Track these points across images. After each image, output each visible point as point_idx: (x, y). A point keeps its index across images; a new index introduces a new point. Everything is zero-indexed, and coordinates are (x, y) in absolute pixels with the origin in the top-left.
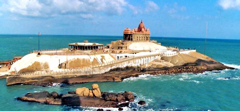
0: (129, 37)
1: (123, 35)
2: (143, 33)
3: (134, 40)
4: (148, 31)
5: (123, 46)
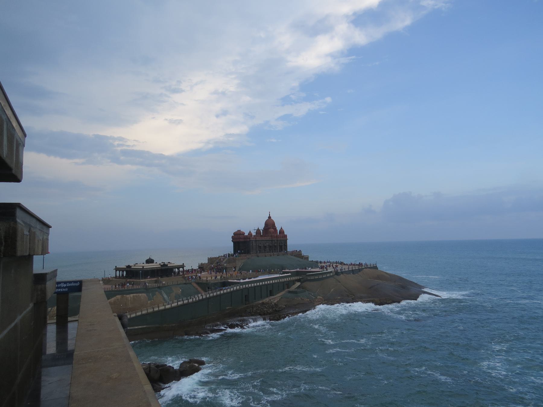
1: (232, 244)
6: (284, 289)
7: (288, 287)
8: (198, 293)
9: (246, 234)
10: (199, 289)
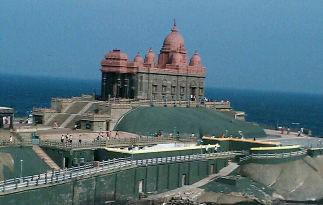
0: (124, 83)
2: (175, 72)
3: (139, 97)
4: (196, 64)
5: (96, 118)
6: (208, 174)
7: (216, 171)
8: (46, 168)
9: (131, 60)
10: (49, 161)
